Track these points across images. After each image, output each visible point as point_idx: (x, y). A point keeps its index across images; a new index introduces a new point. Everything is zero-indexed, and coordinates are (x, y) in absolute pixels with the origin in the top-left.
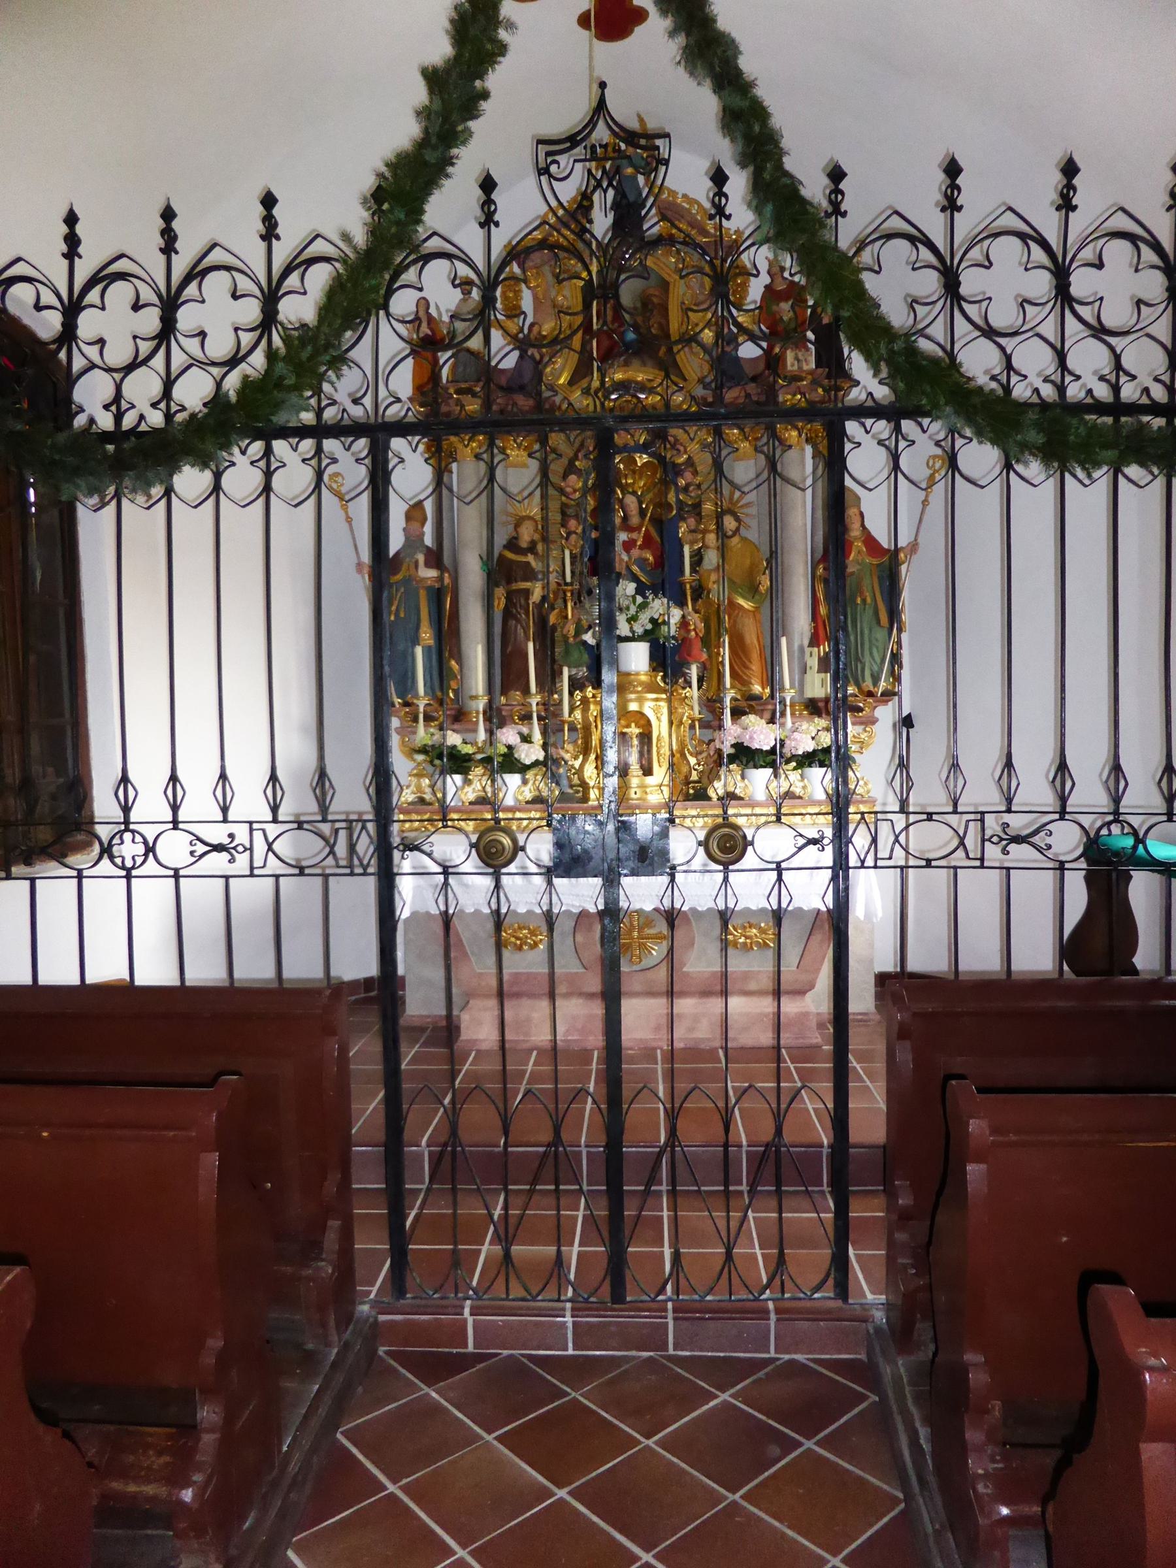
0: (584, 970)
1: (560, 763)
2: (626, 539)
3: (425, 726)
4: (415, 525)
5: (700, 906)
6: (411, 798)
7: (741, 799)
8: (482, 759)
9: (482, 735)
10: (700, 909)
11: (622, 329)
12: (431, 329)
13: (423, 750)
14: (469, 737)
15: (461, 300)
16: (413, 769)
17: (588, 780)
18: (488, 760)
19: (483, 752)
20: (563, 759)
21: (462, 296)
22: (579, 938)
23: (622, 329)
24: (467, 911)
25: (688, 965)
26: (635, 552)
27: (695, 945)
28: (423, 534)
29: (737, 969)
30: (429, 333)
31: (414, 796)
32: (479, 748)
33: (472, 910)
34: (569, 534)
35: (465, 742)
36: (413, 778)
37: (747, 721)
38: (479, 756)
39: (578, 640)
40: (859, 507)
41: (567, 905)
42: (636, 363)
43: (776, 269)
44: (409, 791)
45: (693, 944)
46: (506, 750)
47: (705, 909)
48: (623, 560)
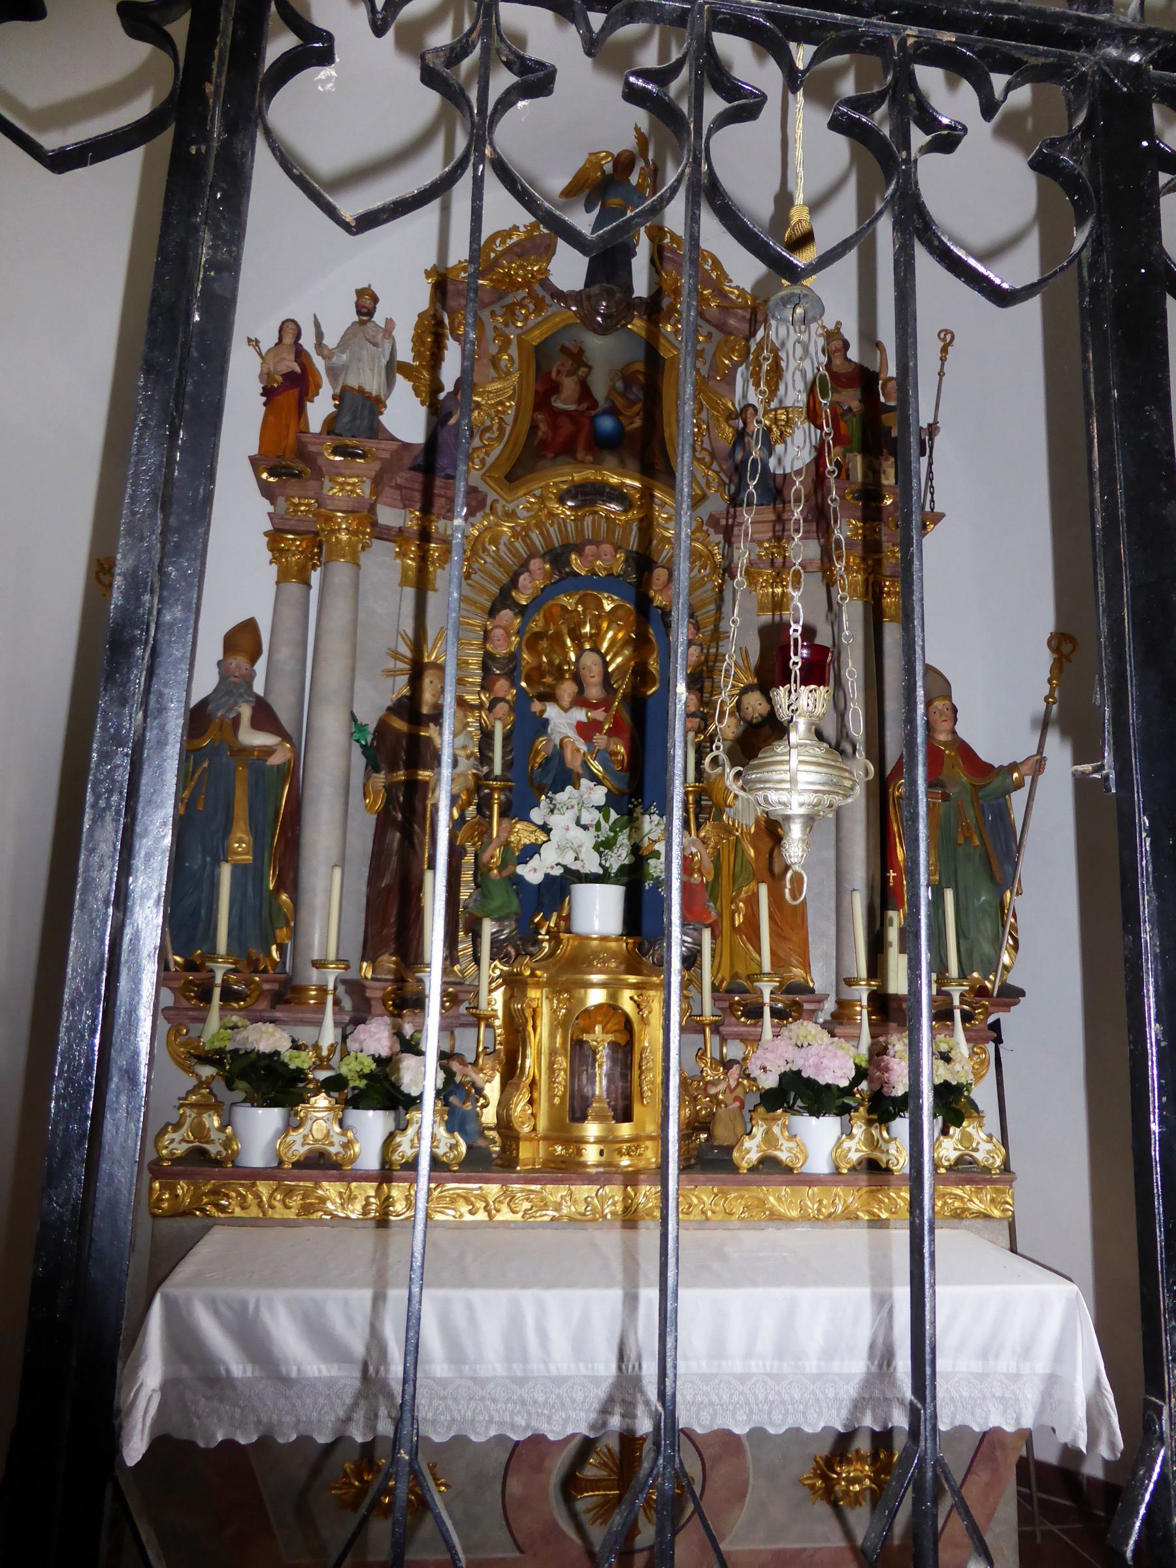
0: (517, 1554)
1: (469, 1092)
2: (584, 719)
3: (222, 1008)
4: (239, 662)
5: (772, 1424)
6: (180, 1149)
7: (789, 1170)
8: (327, 1080)
9: (329, 1035)
10: (772, 1431)
11: (593, 413)
12: (301, 365)
13: (213, 1058)
14: (305, 1034)
15: (354, 324)
16: (189, 1093)
17: (516, 1123)
18: (334, 1085)
19: (330, 1068)
20: (473, 1085)
21: (356, 319)
22: (515, 1486)
23: (593, 413)
24: (281, 1440)
25: (728, 1538)
26: (600, 740)
27: (747, 1499)
28: (251, 676)
29: (824, 1545)
30: (298, 369)
31: (185, 1146)
32: (319, 1057)
33: (294, 1437)
34: (494, 702)
35: (296, 1046)
36: (188, 1112)
37: (802, 1032)
38: (323, 1075)
39: (506, 873)
40: (949, 697)
41: (502, 1423)
42: (611, 460)
43: (837, 344)
44: (177, 1136)
45: (744, 1496)
46: (374, 1066)
47: (782, 1430)
48: (578, 750)
